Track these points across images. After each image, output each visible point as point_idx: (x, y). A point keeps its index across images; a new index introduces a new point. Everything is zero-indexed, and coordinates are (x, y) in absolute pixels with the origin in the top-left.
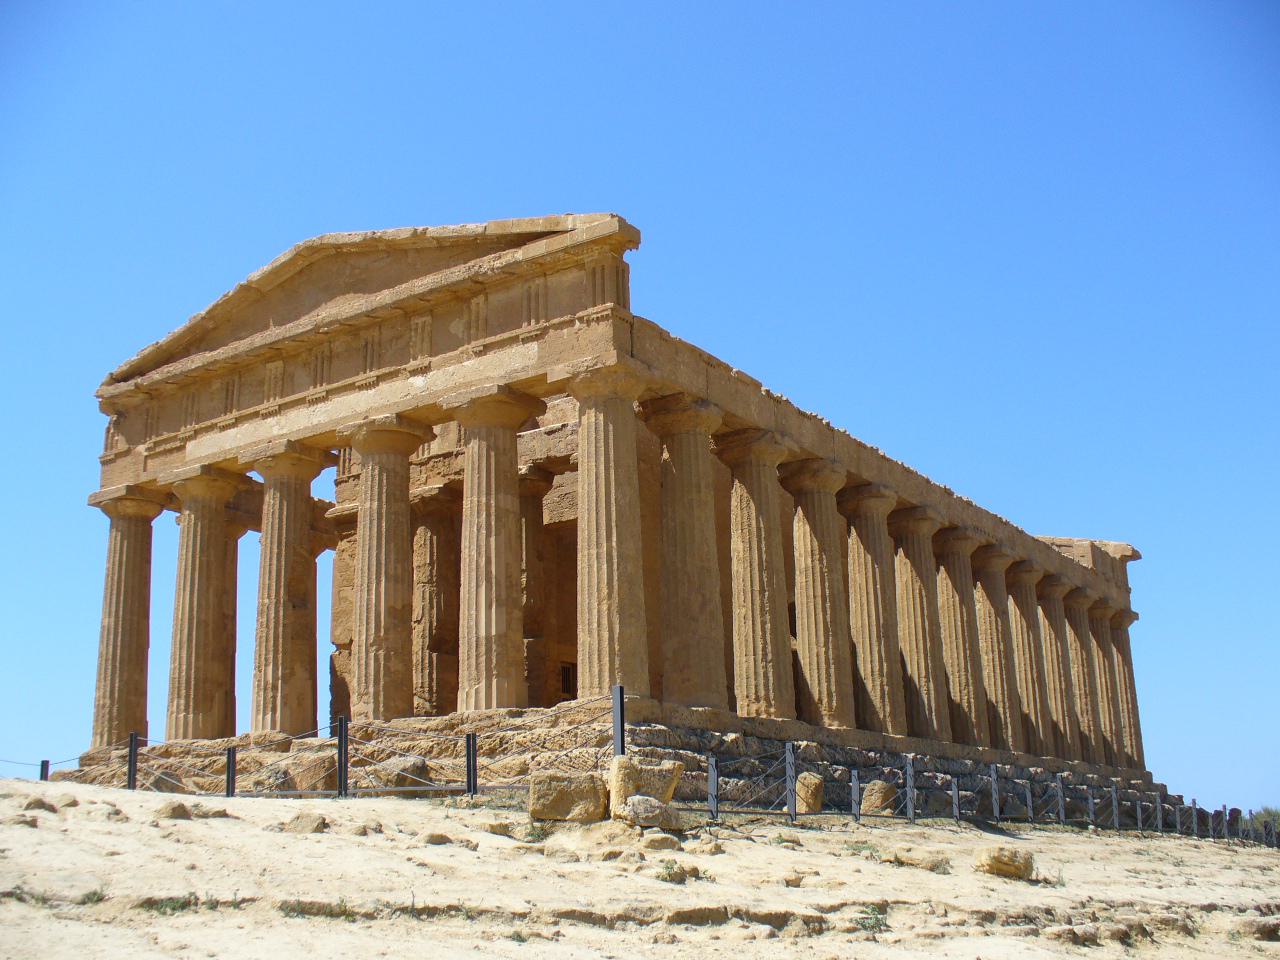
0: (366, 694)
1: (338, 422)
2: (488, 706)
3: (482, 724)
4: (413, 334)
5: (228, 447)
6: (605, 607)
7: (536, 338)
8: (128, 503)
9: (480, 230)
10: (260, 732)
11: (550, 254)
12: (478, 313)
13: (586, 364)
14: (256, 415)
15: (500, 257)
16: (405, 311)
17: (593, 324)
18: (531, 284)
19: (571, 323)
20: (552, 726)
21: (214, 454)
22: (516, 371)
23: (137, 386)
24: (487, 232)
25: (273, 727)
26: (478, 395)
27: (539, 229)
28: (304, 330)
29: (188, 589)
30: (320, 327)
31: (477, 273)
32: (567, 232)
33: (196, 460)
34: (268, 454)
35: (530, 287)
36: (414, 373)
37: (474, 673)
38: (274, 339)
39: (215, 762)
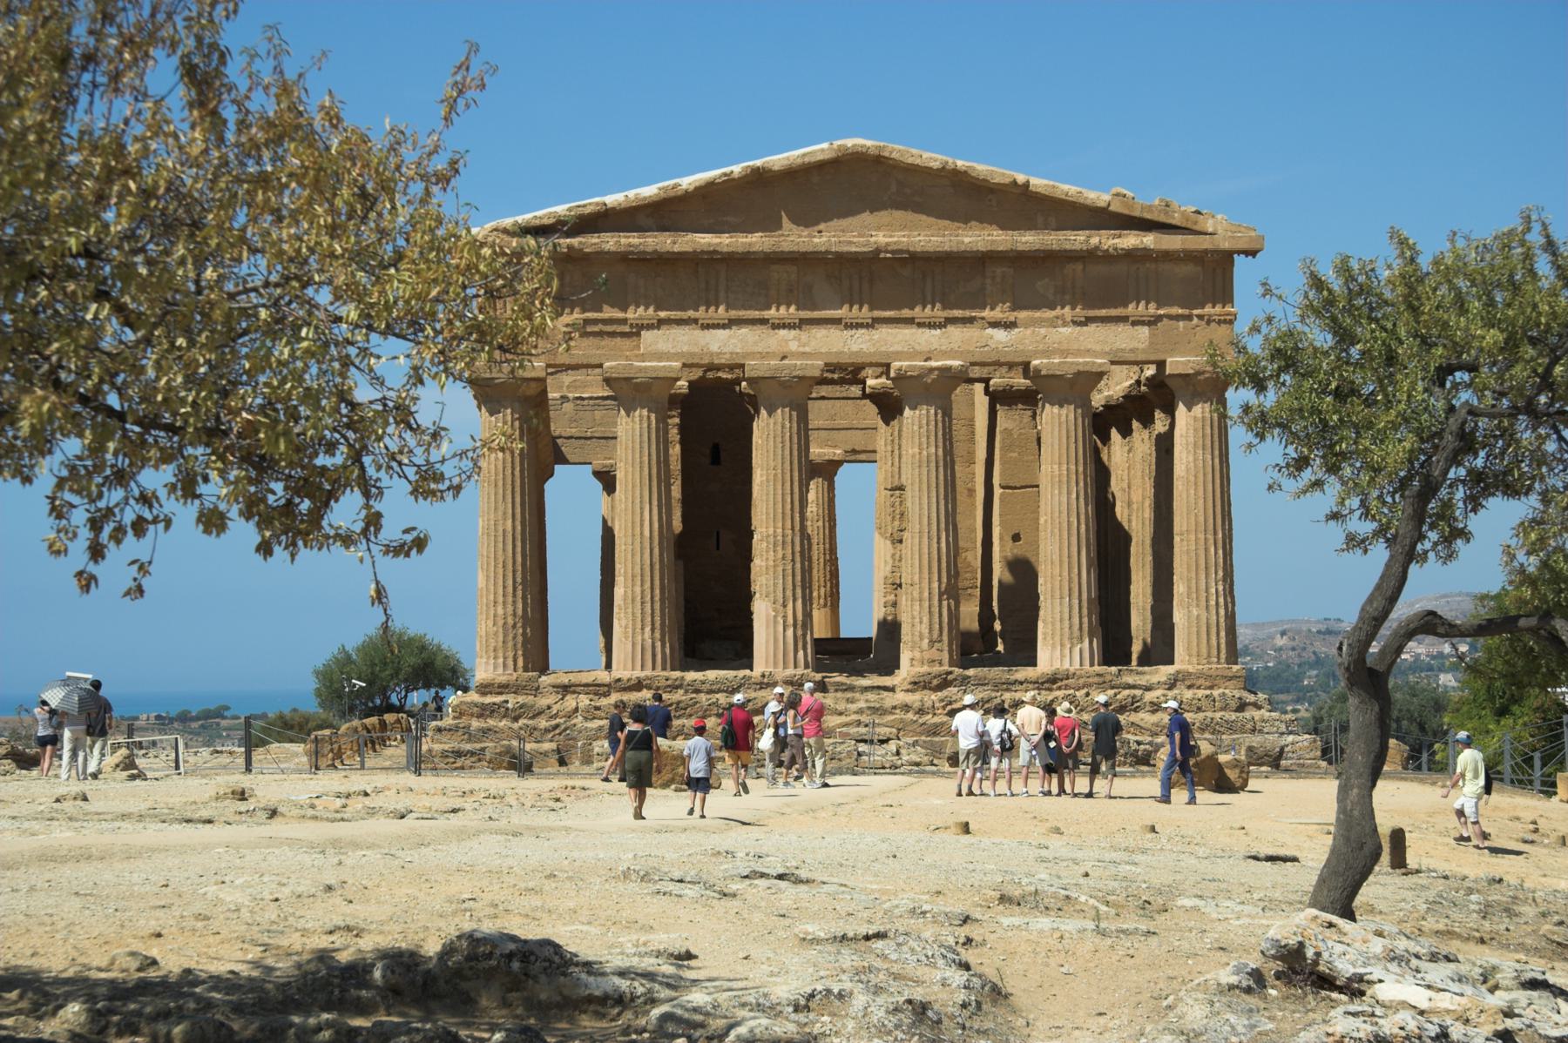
1: (888, 354)
2: (1092, 664)
3: (1091, 680)
4: (988, 281)
5: (714, 348)
6: (1221, 588)
7: (1149, 324)
8: (533, 385)
9: (1102, 204)
10: (790, 671)
14: (763, 322)
15: (1120, 236)
16: (982, 261)
17: (1213, 324)
19: (1189, 318)
20: (1169, 689)
21: (692, 355)
22: (1123, 350)
23: (570, 247)
24: (1111, 208)
25: (806, 667)
28: (858, 250)
29: (655, 503)
30: (881, 251)
31: (1097, 248)
32: (1206, 234)
33: (660, 356)
34: (794, 374)
36: (995, 324)
37: (1076, 633)
38: (811, 249)
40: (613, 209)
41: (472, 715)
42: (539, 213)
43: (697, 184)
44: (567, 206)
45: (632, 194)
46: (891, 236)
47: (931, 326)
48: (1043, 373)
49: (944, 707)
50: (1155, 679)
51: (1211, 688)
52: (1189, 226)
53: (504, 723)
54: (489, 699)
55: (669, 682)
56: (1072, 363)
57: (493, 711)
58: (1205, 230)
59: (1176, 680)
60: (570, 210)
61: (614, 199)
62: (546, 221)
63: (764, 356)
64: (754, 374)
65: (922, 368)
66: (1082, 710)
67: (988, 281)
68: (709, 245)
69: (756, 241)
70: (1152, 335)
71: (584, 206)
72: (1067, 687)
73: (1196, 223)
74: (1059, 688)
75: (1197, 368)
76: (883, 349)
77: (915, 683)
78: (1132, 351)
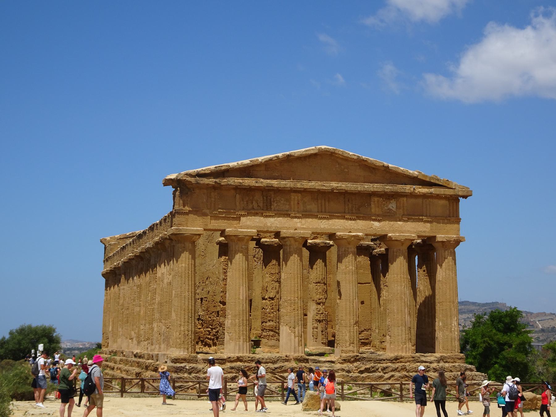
0: (353, 343)
5: (269, 224)
11: (444, 194)
12: (403, 203)
13: (453, 238)
18: (425, 200)
21: (260, 227)
23: (215, 182)
24: (418, 177)
26: (409, 238)
27: (441, 184)
28: (326, 188)
35: (426, 201)
38: (308, 187)
39: (283, 367)
40: (233, 168)
41: (172, 372)
42: (204, 168)
43: (266, 160)
44: (214, 166)
45: (240, 162)
46: (338, 184)
47: (351, 219)
48: (393, 239)
49: (357, 370)
50: (432, 359)
51: (452, 363)
52: (446, 185)
53: (186, 375)
54: (178, 365)
55: (250, 359)
56: (404, 236)
57: (181, 370)
58: (452, 187)
59: (440, 360)
60: (216, 167)
61: (233, 164)
62: (207, 172)
63: (288, 228)
64: (284, 235)
65: (348, 235)
66: (408, 371)
67: (372, 203)
68: (270, 184)
69: (287, 184)
70: (431, 226)
71: (222, 166)
72: (401, 362)
73: (449, 184)
74: (398, 362)
75: (448, 239)
76: (333, 227)
77: (344, 360)
78: (424, 232)
